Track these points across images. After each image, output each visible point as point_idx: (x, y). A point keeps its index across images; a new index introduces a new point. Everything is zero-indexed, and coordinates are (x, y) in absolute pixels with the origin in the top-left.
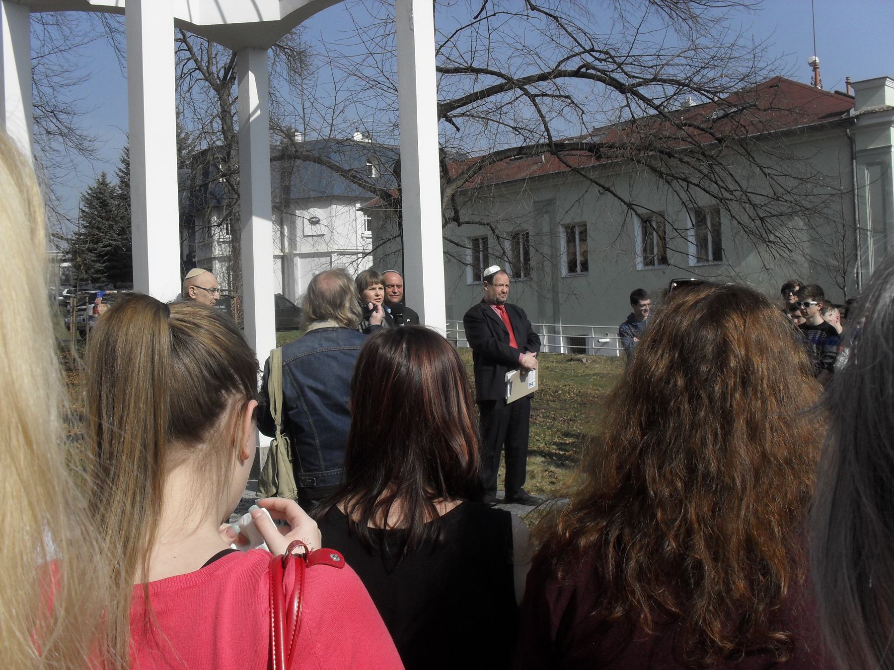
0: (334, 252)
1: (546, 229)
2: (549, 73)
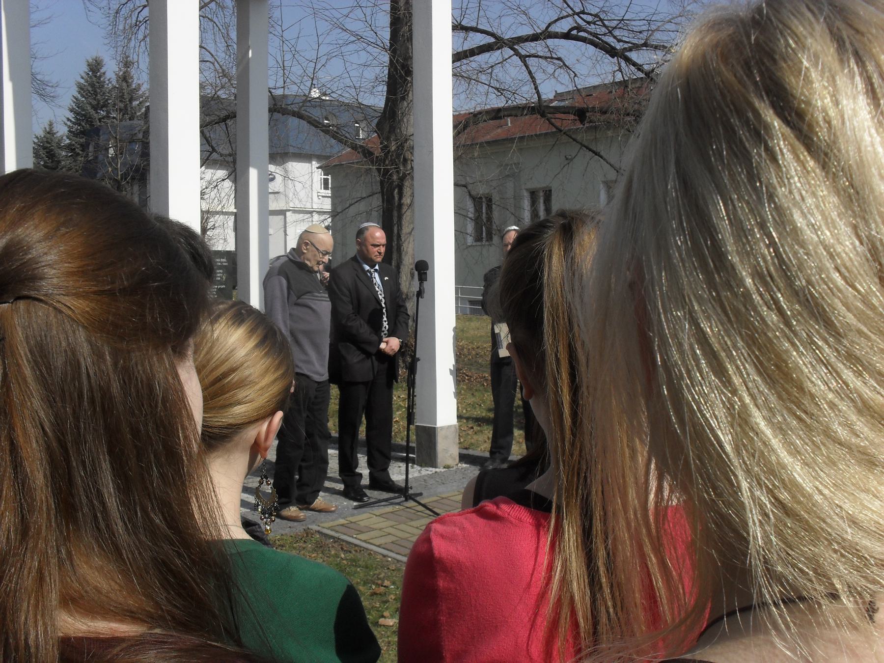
0: (289, 210)
1: (510, 193)
2: (541, 34)
